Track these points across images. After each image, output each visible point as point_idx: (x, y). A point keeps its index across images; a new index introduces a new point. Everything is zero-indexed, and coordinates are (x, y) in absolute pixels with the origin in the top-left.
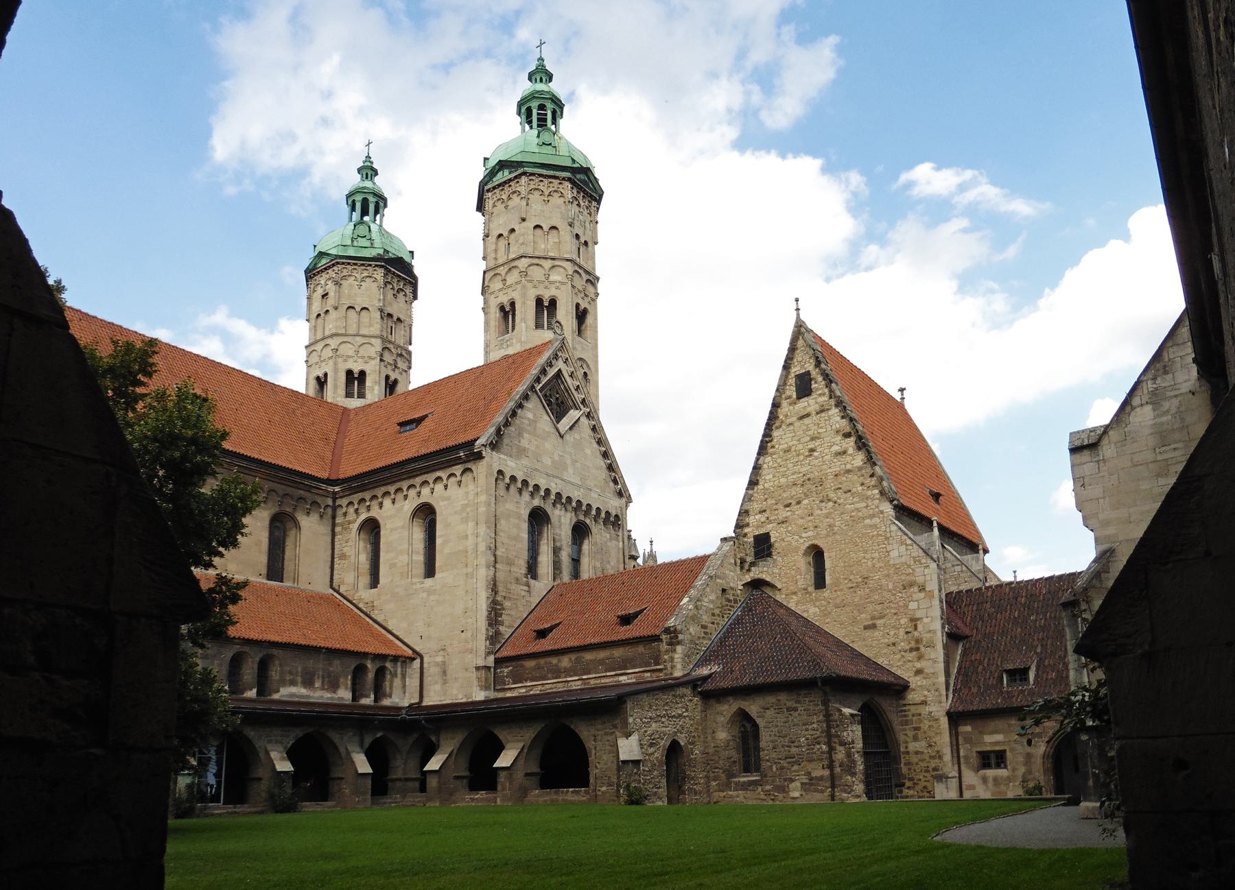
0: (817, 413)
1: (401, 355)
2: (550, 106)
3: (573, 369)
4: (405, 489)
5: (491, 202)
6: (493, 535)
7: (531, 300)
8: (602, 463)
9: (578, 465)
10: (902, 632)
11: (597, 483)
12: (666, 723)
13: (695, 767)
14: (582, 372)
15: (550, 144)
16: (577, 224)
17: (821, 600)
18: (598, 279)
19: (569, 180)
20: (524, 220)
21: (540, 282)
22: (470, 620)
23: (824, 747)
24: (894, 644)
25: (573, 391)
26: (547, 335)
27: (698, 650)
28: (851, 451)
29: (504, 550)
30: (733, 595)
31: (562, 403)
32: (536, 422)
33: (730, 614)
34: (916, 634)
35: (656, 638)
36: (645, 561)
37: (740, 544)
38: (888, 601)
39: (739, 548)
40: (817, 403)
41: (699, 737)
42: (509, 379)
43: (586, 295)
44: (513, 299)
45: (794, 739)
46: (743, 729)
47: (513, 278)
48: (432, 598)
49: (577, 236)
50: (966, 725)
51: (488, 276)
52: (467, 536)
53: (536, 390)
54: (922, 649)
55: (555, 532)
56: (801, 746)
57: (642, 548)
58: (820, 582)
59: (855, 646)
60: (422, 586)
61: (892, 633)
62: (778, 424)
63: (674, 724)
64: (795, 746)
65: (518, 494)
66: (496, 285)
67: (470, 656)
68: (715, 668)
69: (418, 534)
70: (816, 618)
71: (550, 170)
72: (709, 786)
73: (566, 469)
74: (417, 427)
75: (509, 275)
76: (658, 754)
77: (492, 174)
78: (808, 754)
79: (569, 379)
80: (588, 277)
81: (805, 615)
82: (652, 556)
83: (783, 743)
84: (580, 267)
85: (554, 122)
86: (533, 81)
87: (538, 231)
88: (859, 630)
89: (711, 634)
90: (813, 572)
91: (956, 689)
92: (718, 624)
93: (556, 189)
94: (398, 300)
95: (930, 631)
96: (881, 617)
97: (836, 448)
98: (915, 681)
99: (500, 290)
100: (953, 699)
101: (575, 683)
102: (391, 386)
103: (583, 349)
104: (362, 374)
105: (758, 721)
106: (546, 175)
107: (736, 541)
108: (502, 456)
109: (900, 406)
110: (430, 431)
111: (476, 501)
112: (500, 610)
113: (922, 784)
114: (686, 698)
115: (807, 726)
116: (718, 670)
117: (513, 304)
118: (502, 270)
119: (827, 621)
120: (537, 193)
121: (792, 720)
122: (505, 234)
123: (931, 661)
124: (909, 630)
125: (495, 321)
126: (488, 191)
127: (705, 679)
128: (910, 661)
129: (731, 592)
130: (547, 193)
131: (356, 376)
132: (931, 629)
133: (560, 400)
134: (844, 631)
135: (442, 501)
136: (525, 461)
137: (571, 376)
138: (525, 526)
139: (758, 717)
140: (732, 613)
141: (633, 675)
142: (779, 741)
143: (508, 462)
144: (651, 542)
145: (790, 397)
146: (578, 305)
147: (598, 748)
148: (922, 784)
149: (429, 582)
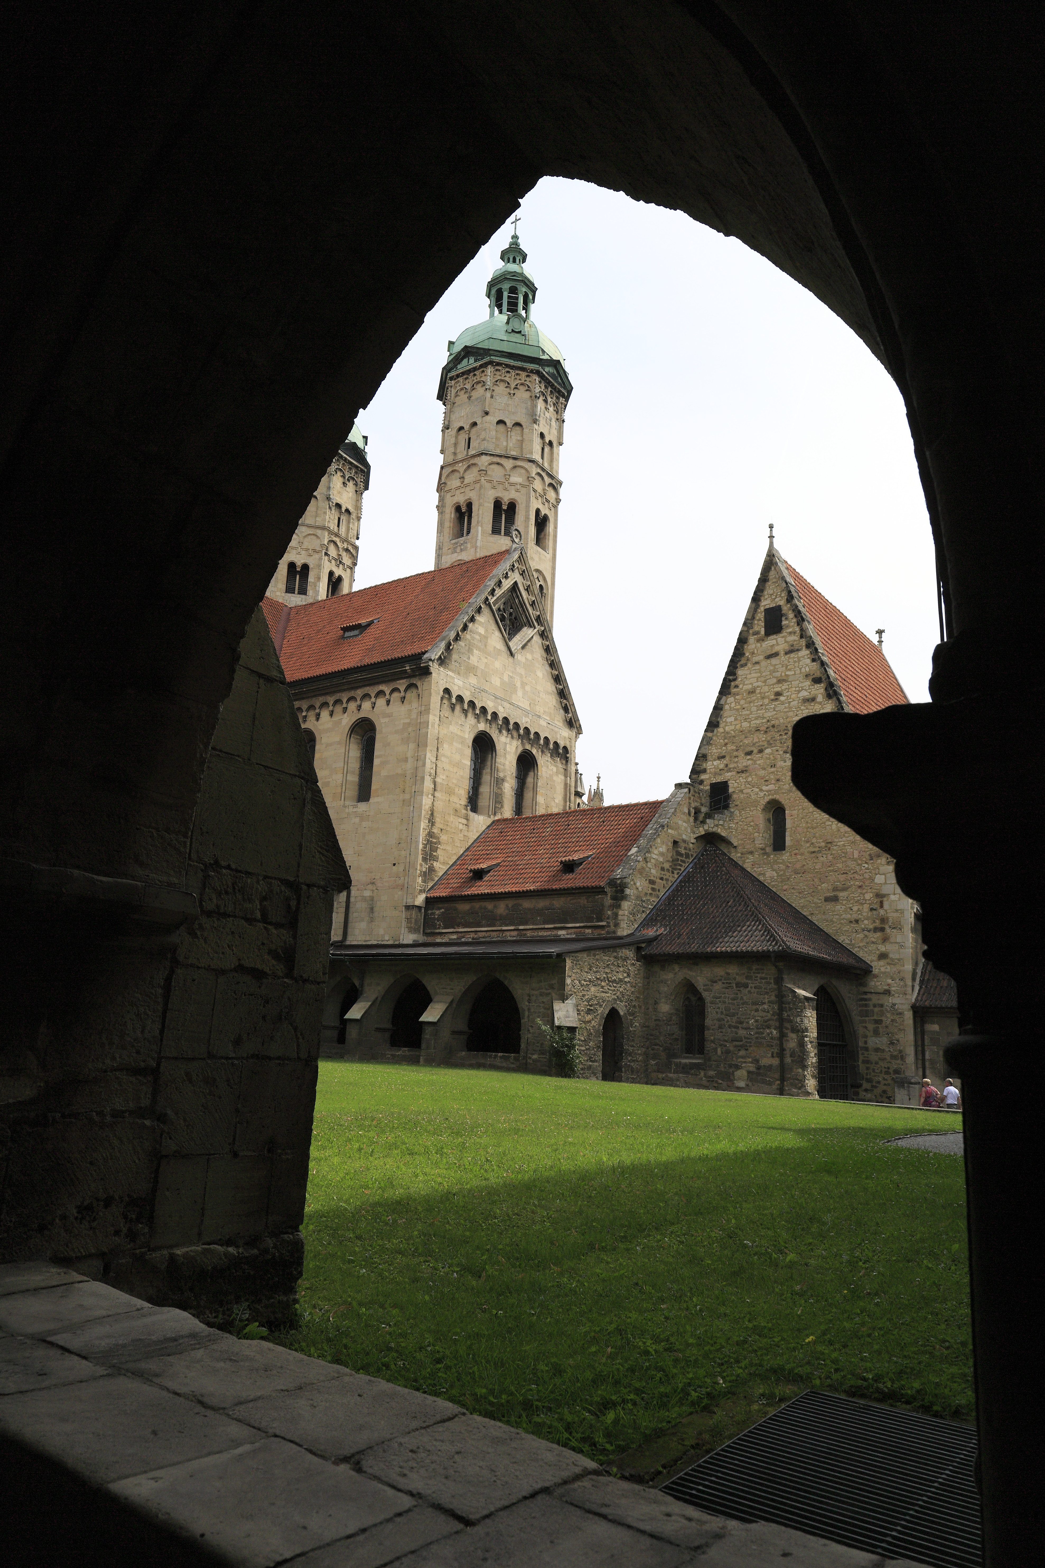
0: (786, 653)
1: (347, 550)
2: (523, 289)
3: (529, 583)
4: (345, 701)
5: (454, 391)
6: (434, 760)
7: (489, 502)
9: (528, 688)
10: (866, 907)
11: (547, 710)
12: (606, 988)
14: (538, 584)
15: (520, 332)
16: (542, 421)
17: (781, 863)
18: (561, 483)
19: (538, 373)
20: (487, 413)
21: (500, 483)
22: (403, 853)
23: (775, 1032)
24: (857, 921)
26: (502, 543)
27: (644, 907)
28: (820, 698)
29: (444, 777)
30: (685, 848)
31: (515, 618)
32: (486, 638)
33: (680, 870)
34: (882, 912)
35: (599, 890)
36: (590, 800)
37: (695, 792)
38: (852, 871)
39: (694, 796)
40: (786, 642)
41: (640, 1007)
42: (461, 589)
44: (470, 499)
45: (742, 1020)
46: (687, 1003)
47: (470, 477)
48: (364, 824)
49: (542, 436)
50: (932, 1023)
51: (446, 471)
52: (407, 758)
54: (888, 930)
56: (749, 1028)
57: (588, 784)
58: (779, 843)
59: (814, 919)
60: (355, 810)
61: (855, 908)
62: (743, 662)
63: (614, 990)
64: (742, 1028)
65: (463, 716)
66: (454, 483)
67: (400, 893)
68: (662, 930)
69: (355, 753)
70: (773, 883)
71: (518, 361)
72: (647, 1065)
73: (514, 689)
74: (361, 633)
75: (468, 472)
76: (596, 1023)
77: (455, 361)
78: (757, 1038)
79: (524, 594)
81: (761, 878)
82: (598, 795)
83: (730, 1023)
84: (543, 470)
85: (526, 308)
86: (506, 260)
87: (501, 427)
88: (819, 902)
89: (659, 891)
90: (772, 831)
91: (923, 979)
92: (667, 880)
93: (523, 381)
94: (348, 489)
95: (897, 911)
96: (844, 889)
97: (804, 694)
98: (878, 967)
99: (458, 488)
100: (919, 991)
101: (510, 932)
102: (335, 583)
103: (540, 559)
104: (305, 568)
105: (705, 994)
106: (513, 366)
107: (692, 788)
108: (450, 673)
109: (876, 651)
110: (376, 639)
111: (419, 721)
113: (882, 1087)
114: (629, 962)
115: (757, 1006)
116: (665, 933)
117: (469, 505)
118: (461, 467)
119: (785, 887)
120: (502, 386)
121: (742, 998)
122: (467, 427)
123: (897, 945)
124: (875, 906)
125: (450, 522)
126: (451, 379)
127: (650, 941)
128: (873, 942)
129: (683, 845)
130: (513, 386)
131: (298, 569)
132: (899, 908)
134: (802, 900)
135: (383, 718)
136: (473, 680)
137: (527, 590)
138: (468, 752)
139: (705, 990)
140: (683, 869)
141: (573, 930)
142: (726, 1020)
143: (456, 680)
144: (599, 778)
145: (757, 633)
146: (538, 511)
147: (532, 1010)
148: (882, 1087)
149: (362, 807)
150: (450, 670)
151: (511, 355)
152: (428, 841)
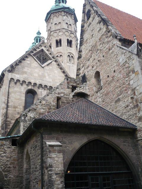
3: (48, 49)
8: (63, 75)
13: (9, 185)
19: (63, 11)
20: (52, 23)
24: (128, 106)
25: (49, 55)
29: (12, 103)
31: (45, 59)
32: (31, 64)
43: (70, 37)
49: (67, 23)
53: (31, 55)
55: (39, 97)
65: (21, 86)
73: (45, 77)
80: (71, 32)
87: (56, 25)
103: (70, 50)
108: (14, 74)
112: (9, 124)
120: (55, 17)
130: (57, 16)
133: (44, 58)
136: (25, 76)
138: (24, 95)
150: (14, 73)
151: (55, 10)
152: (4, 123)
